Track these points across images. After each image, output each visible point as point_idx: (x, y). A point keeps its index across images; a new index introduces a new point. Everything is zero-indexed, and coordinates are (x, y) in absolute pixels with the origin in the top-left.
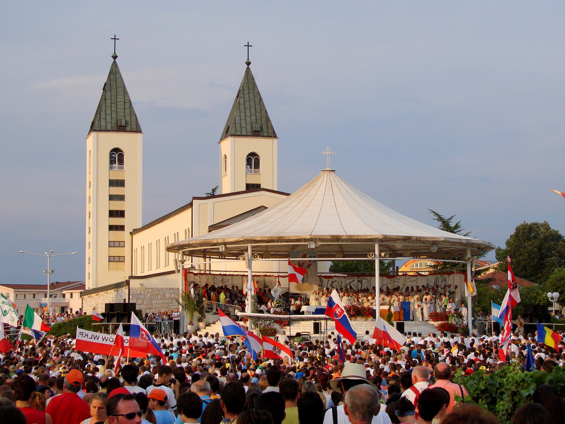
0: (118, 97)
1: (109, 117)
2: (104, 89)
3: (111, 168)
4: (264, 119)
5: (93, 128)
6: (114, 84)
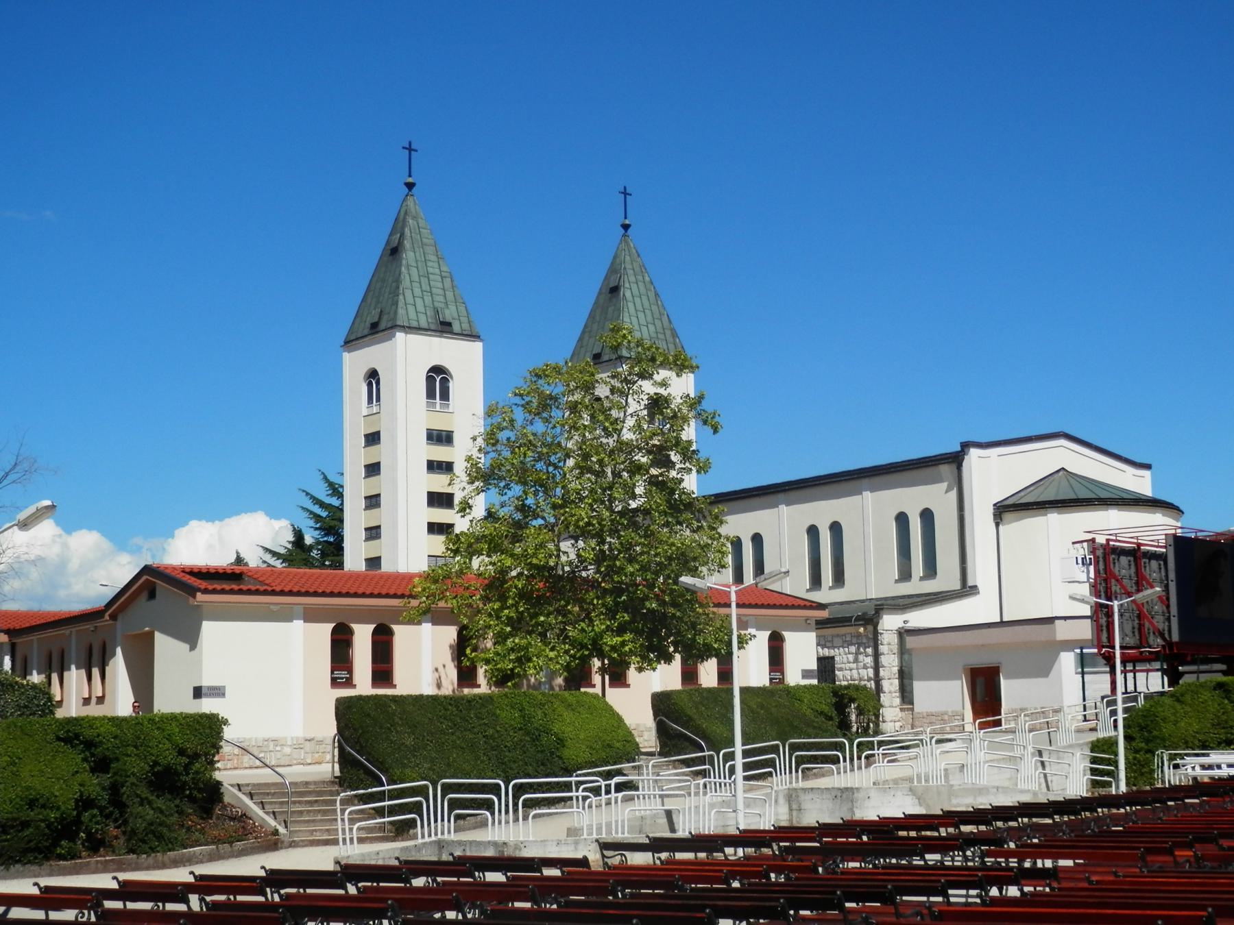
0: (430, 264)
4: (668, 333)
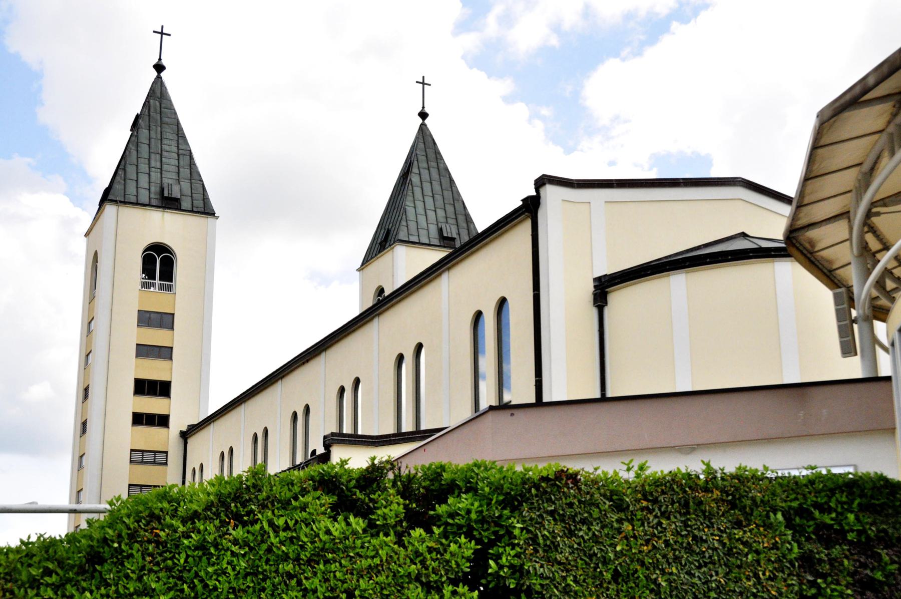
0: (165, 142)
2: (135, 126)
3: (145, 285)
4: (461, 219)
5: (106, 198)
6: (157, 118)
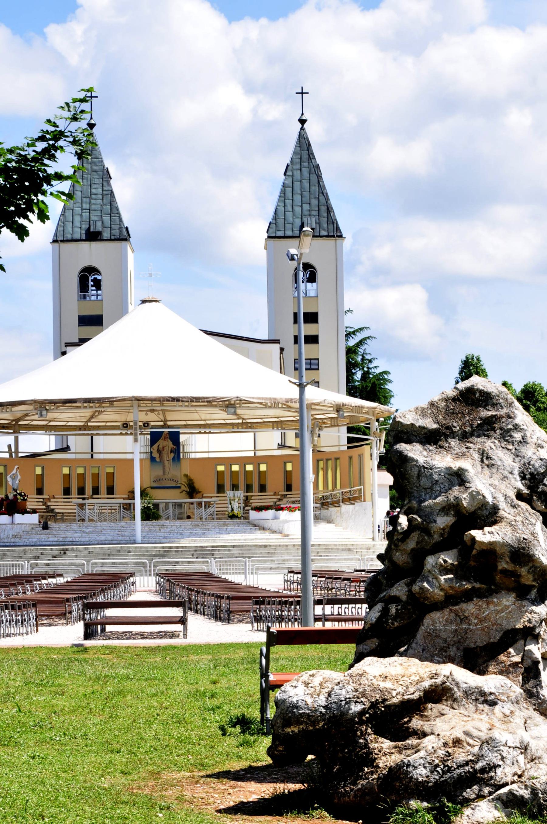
0: (94, 186)
1: (77, 219)
4: (323, 209)
